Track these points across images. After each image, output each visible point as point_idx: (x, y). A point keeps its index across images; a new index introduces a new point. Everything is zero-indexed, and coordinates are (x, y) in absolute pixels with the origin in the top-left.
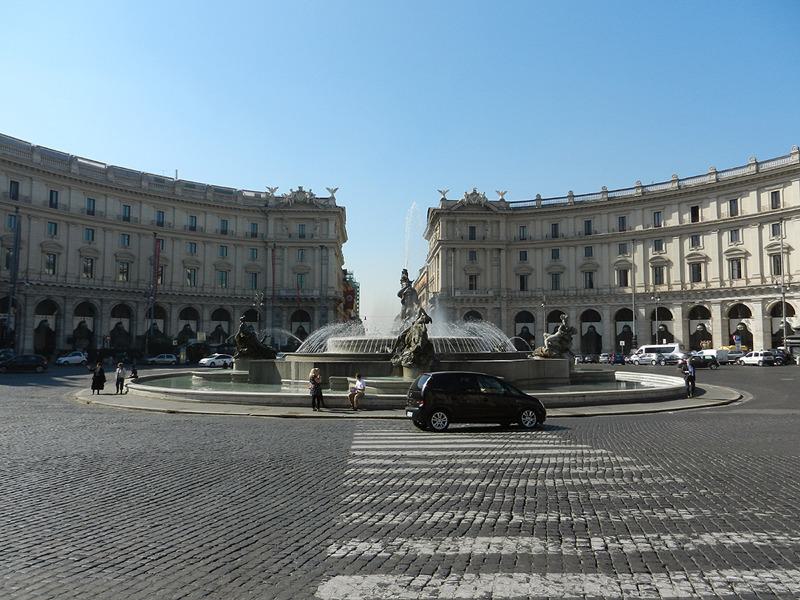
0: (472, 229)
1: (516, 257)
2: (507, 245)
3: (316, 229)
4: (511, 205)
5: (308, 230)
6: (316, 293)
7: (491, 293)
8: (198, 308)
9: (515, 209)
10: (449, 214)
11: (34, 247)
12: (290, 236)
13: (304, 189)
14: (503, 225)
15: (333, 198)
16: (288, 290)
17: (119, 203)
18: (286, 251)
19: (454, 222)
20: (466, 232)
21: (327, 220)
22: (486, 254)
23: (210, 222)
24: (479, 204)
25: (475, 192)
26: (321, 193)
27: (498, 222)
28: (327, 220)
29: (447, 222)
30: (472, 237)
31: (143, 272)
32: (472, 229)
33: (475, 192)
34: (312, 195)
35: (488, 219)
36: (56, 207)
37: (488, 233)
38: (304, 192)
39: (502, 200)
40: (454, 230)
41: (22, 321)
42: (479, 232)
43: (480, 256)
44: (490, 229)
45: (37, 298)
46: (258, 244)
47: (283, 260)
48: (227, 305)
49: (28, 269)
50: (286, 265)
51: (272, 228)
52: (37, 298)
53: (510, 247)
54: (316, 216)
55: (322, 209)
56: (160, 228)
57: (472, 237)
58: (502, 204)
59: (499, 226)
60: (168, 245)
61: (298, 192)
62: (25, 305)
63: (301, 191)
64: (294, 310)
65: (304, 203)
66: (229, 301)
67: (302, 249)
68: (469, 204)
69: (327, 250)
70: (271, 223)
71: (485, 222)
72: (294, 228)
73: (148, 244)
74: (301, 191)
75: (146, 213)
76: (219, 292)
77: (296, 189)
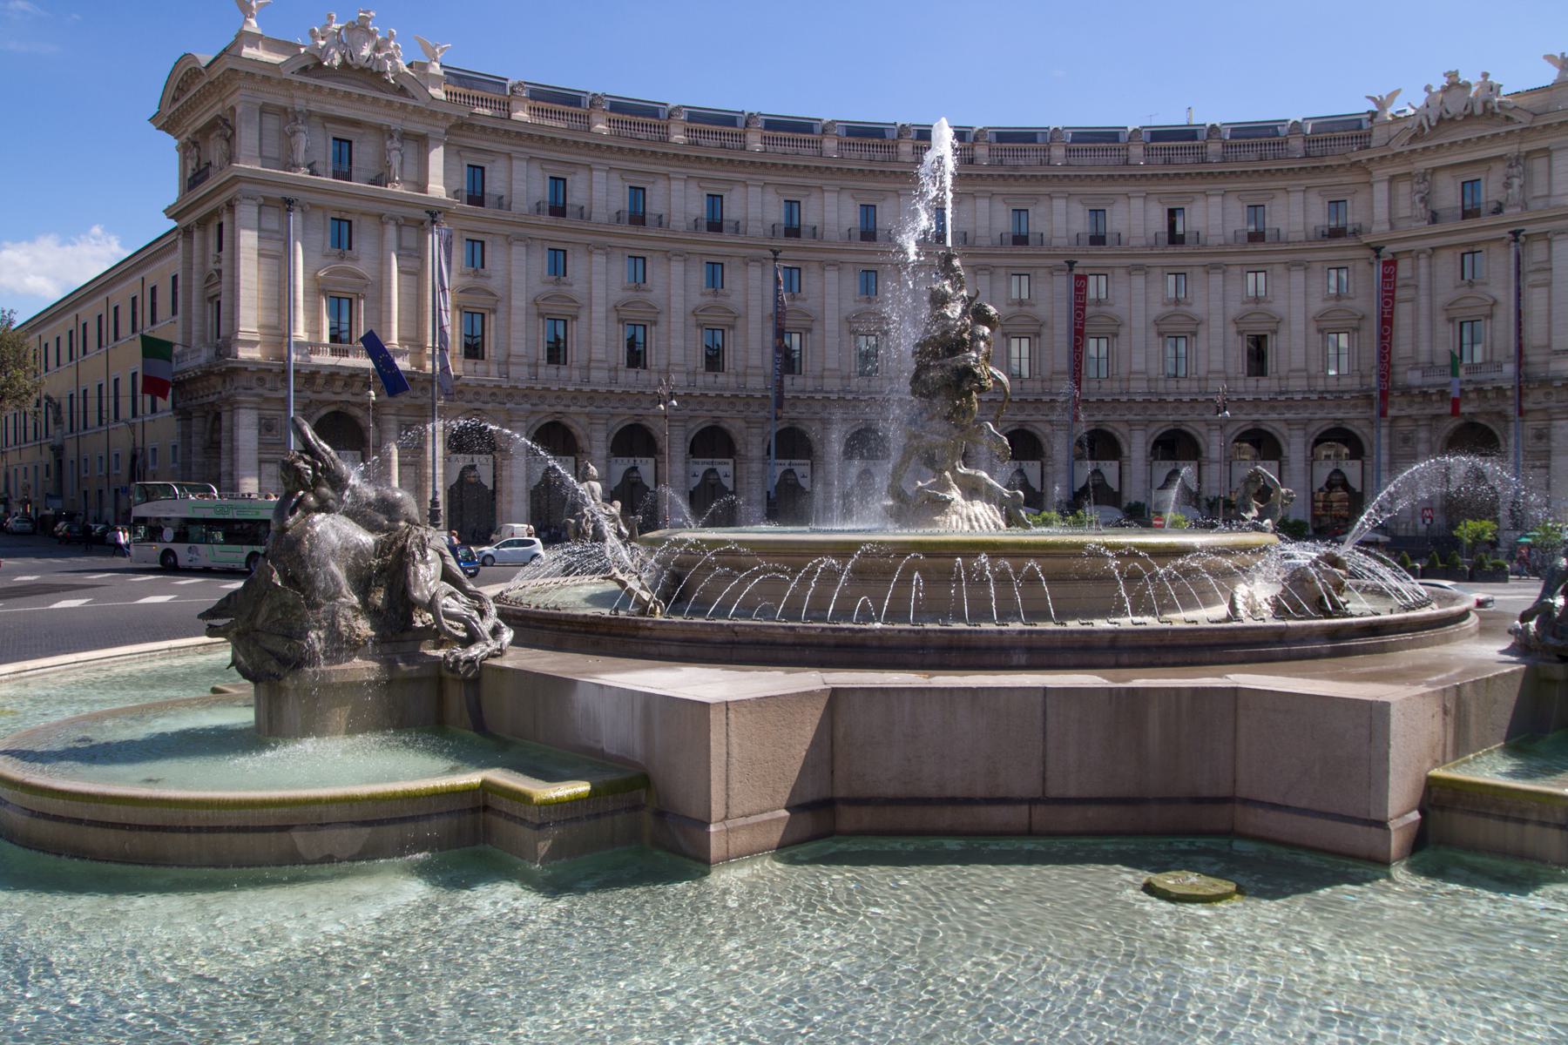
3: (1507, 185)
8: (1195, 428)
12: (1434, 218)
13: (1464, 77)
18: (1423, 262)
23: (1213, 216)
28: (1547, 152)
38: (1467, 86)
46: (1350, 254)
47: (1416, 287)
48: (1272, 421)
50: (1423, 300)
51: (1378, 208)
61: (1445, 90)
63: (1454, 84)
66: (1273, 408)
67: (1471, 250)
69: (1550, 241)
70: (1381, 191)
74: (1454, 84)
76: (1249, 386)
77: (1439, 83)
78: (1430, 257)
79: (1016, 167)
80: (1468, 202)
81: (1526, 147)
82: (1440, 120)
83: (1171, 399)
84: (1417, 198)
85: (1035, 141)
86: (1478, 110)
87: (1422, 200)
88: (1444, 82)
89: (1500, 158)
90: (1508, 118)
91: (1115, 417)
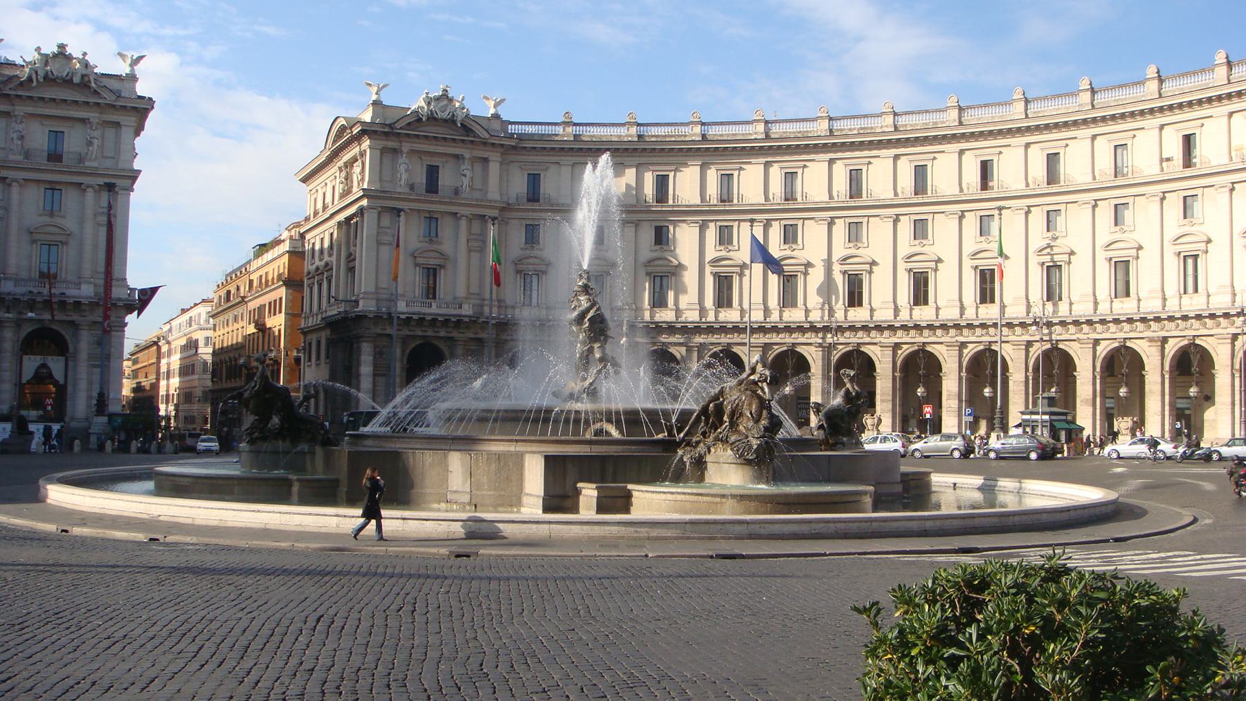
0: (433, 172)
1: (517, 237)
2: (503, 209)
3: (90, 143)
4: (512, 129)
5: (73, 141)
6: (87, 291)
7: (467, 310)
9: (521, 137)
10: (385, 134)
13: (69, 50)
14: (494, 168)
15: (132, 78)
16: (17, 281)
19: (395, 152)
20: (421, 178)
21: (117, 125)
22: (457, 227)
24: (451, 121)
25: (445, 96)
26: (106, 63)
27: (485, 160)
28: (117, 125)
29: (384, 151)
30: (432, 185)
32: (433, 172)
33: (445, 96)
34: (86, 65)
35: (467, 154)
37: (466, 181)
38: (69, 58)
39: (496, 116)
40: (394, 170)
42: (446, 179)
43: (446, 228)
44: (468, 173)
53: (507, 214)
54: (93, 115)
55: (110, 98)
57: (432, 185)
58: (496, 125)
61: (55, 56)
63: (62, 54)
64: (27, 329)
65: (67, 82)
67: (53, 187)
68: (432, 118)
71: (457, 157)
72: (38, 137)
74: (62, 54)
78: (21, 186)
80: (52, 147)
82: (46, 77)
84: (15, 136)
86: (76, 80)
87: (22, 138)
88: (55, 50)
89: (83, 121)
90: (96, 92)
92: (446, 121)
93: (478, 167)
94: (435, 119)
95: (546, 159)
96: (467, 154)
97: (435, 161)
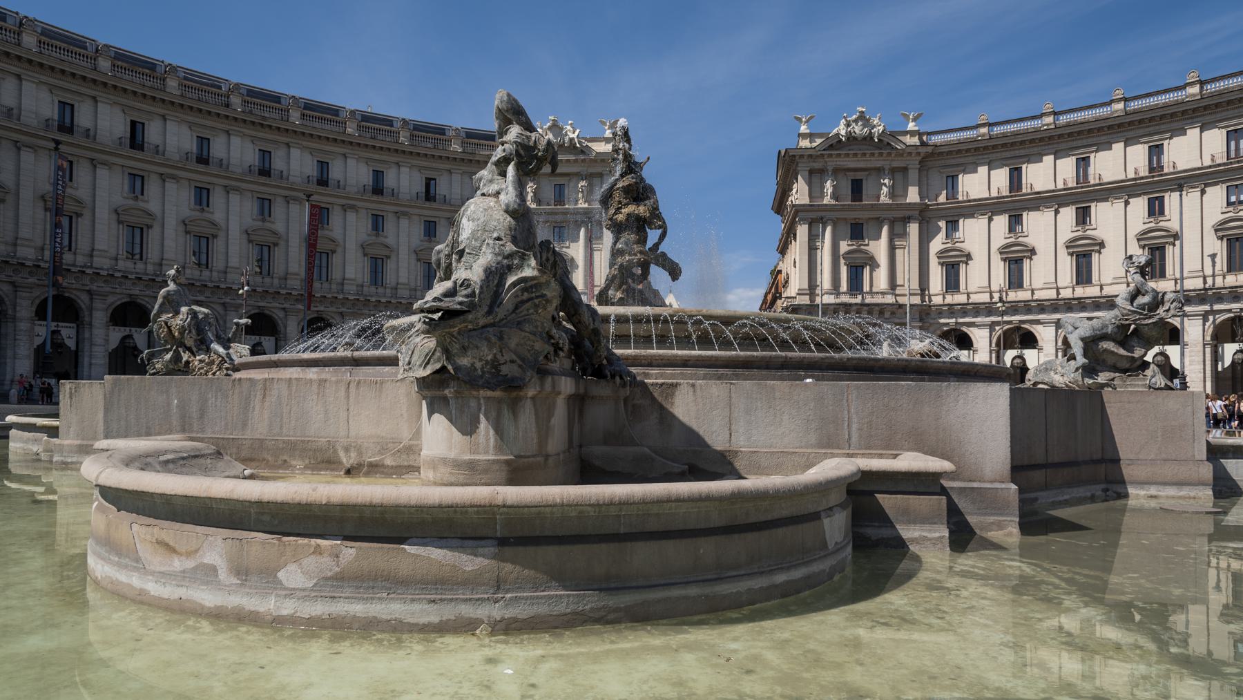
11: (103, 214)
17: (251, 145)
27: (905, 170)
31: (292, 259)
36: (142, 148)
41: (87, 335)
45: (111, 299)
49: (93, 250)
52: (111, 299)
56: (321, 189)
59: (906, 177)
60: (336, 219)
62: (91, 309)
68: (851, 138)
73: (300, 216)
75: (298, 164)
79: (265, 118)
81: (591, 170)
83: (373, 299)
85: (279, 103)
91: (333, 309)
92: (865, 138)
93: (899, 176)
94: (855, 138)
95: (962, 160)
96: (887, 167)
97: (859, 175)
